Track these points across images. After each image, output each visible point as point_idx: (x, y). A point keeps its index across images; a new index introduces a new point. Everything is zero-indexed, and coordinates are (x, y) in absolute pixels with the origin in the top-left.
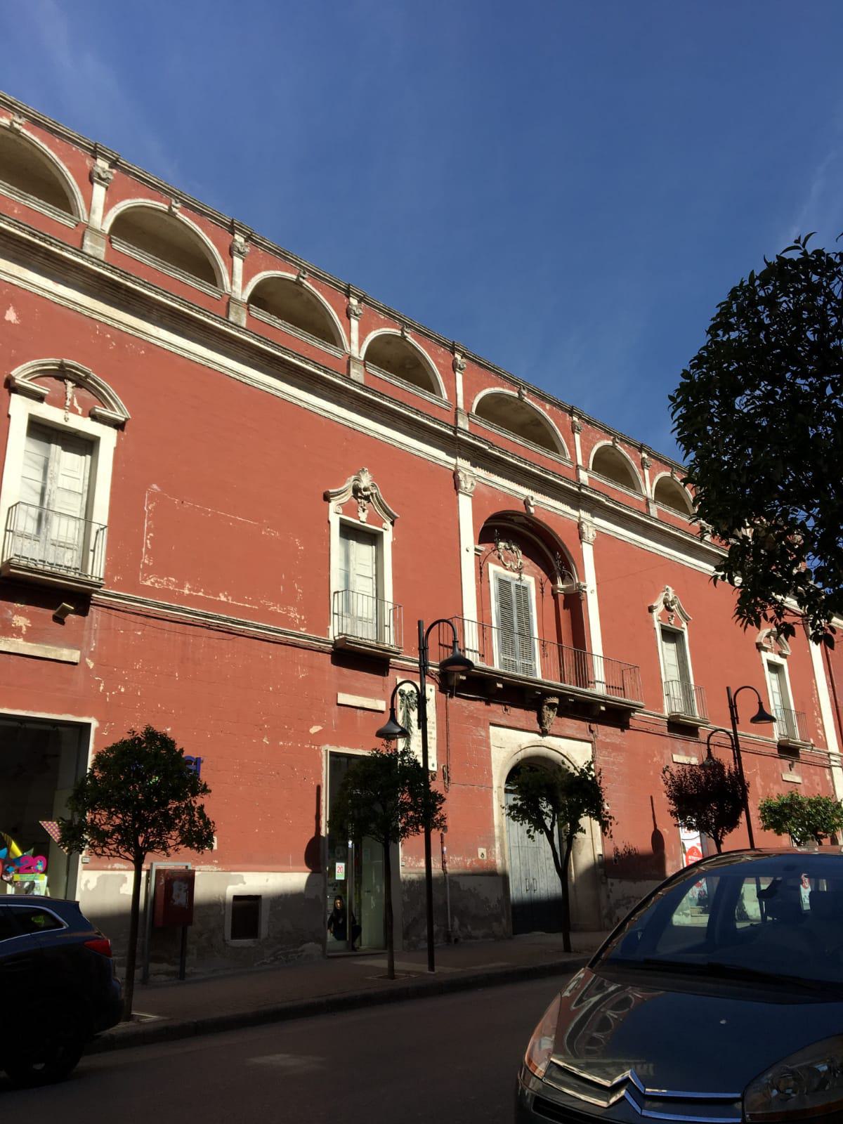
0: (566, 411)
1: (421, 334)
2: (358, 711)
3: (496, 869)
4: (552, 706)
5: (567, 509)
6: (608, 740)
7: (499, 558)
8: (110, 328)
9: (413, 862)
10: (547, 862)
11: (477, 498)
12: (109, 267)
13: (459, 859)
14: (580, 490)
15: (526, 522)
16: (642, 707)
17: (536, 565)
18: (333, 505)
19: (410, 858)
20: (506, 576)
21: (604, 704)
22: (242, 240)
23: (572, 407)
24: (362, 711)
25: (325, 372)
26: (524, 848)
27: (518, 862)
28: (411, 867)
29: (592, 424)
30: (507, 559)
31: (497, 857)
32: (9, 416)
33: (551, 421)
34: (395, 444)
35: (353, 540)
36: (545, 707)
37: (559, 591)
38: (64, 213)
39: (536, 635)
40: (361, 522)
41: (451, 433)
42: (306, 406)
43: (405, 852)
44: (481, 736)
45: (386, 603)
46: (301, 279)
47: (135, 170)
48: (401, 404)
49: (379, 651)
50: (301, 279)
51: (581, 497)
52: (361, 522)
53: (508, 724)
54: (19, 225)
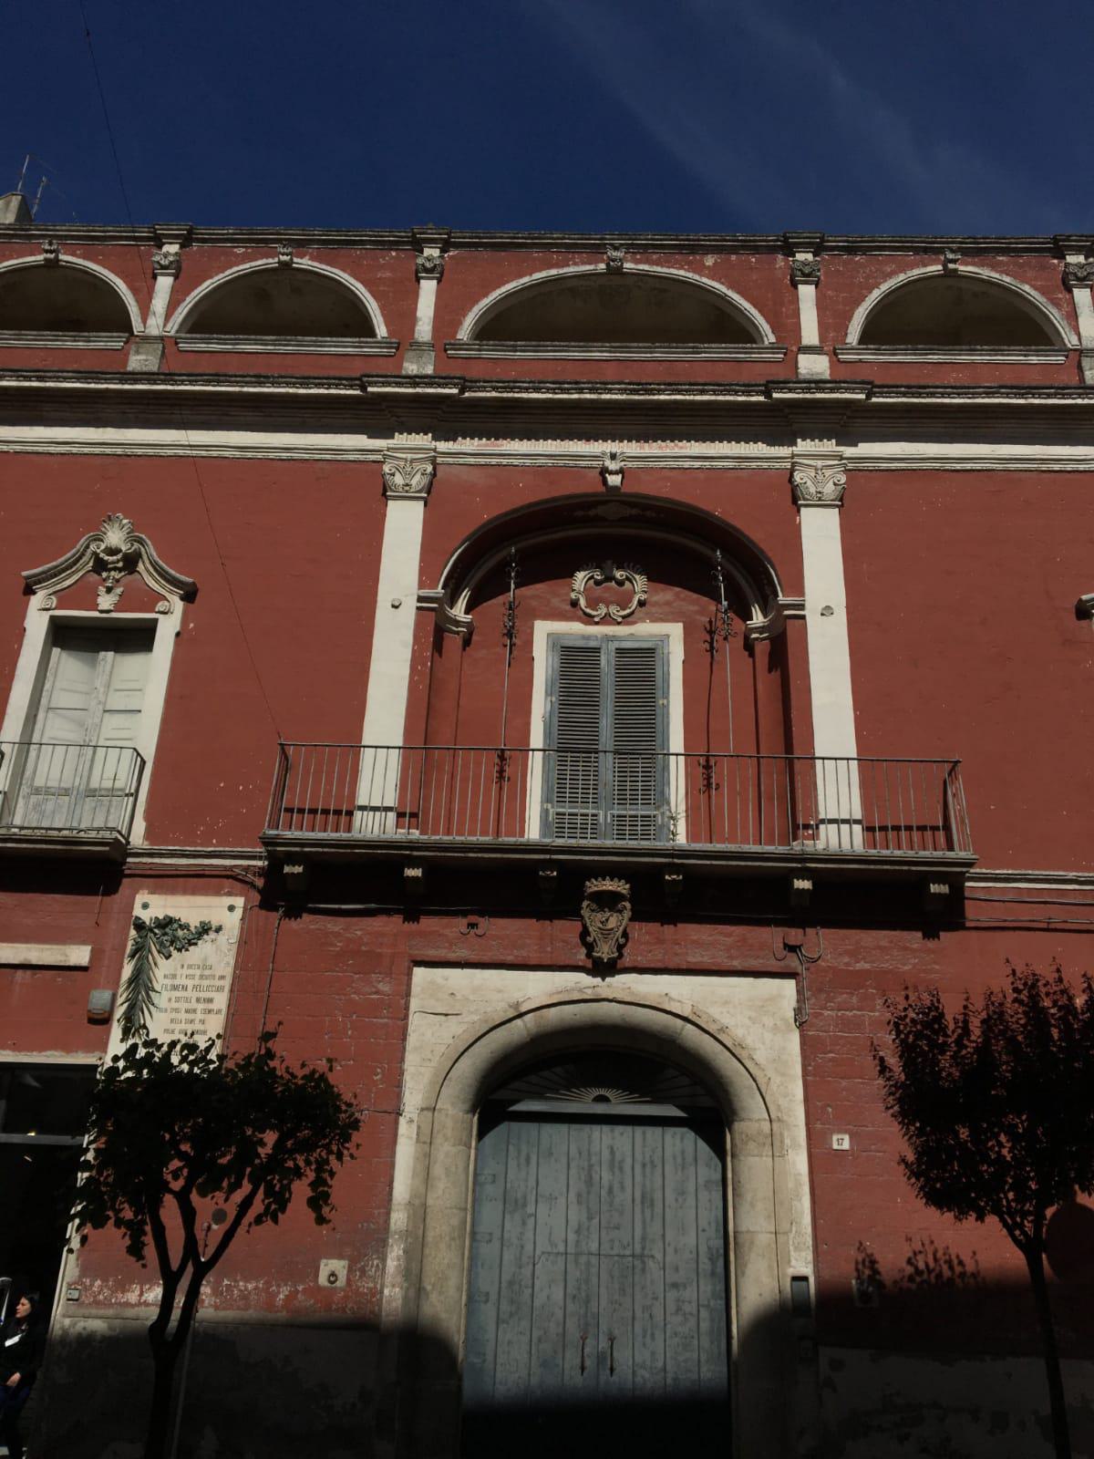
0: (772, 250)
1: (975, 252)
2: (20, 973)
3: (378, 1315)
4: (607, 901)
5: (759, 449)
6: (859, 966)
7: (575, 604)
8: (275, 462)
9: (107, 1292)
10: (672, 1295)
11: (430, 494)
12: (70, 374)
13: (250, 1286)
14: (768, 395)
15: (634, 512)
16: (971, 865)
17: (695, 596)
18: (36, 601)
19: (98, 1282)
20: (587, 638)
21: (804, 874)
22: (810, 257)
23: (1054, 238)
24: (29, 972)
25: (40, 379)
26: (583, 1259)
27: (558, 1294)
28: (97, 1303)
29: (864, 251)
30: (593, 603)
31: (388, 1280)
32: (25, 629)
33: (538, 276)
34: (226, 454)
35: (107, 650)
36: (585, 904)
37: (754, 636)
38: (595, 344)
39: (676, 742)
40: (102, 612)
41: (358, 392)
42: (18, 448)
43: (86, 1269)
44: (377, 992)
45: (819, 762)
46: (951, 266)
47: (110, 232)
48: (217, 378)
49: (885, 867)
50: (951, 266)
51: (787, 411)
52: (102, 612)
53: (473, 958)
54: (928, 390)
